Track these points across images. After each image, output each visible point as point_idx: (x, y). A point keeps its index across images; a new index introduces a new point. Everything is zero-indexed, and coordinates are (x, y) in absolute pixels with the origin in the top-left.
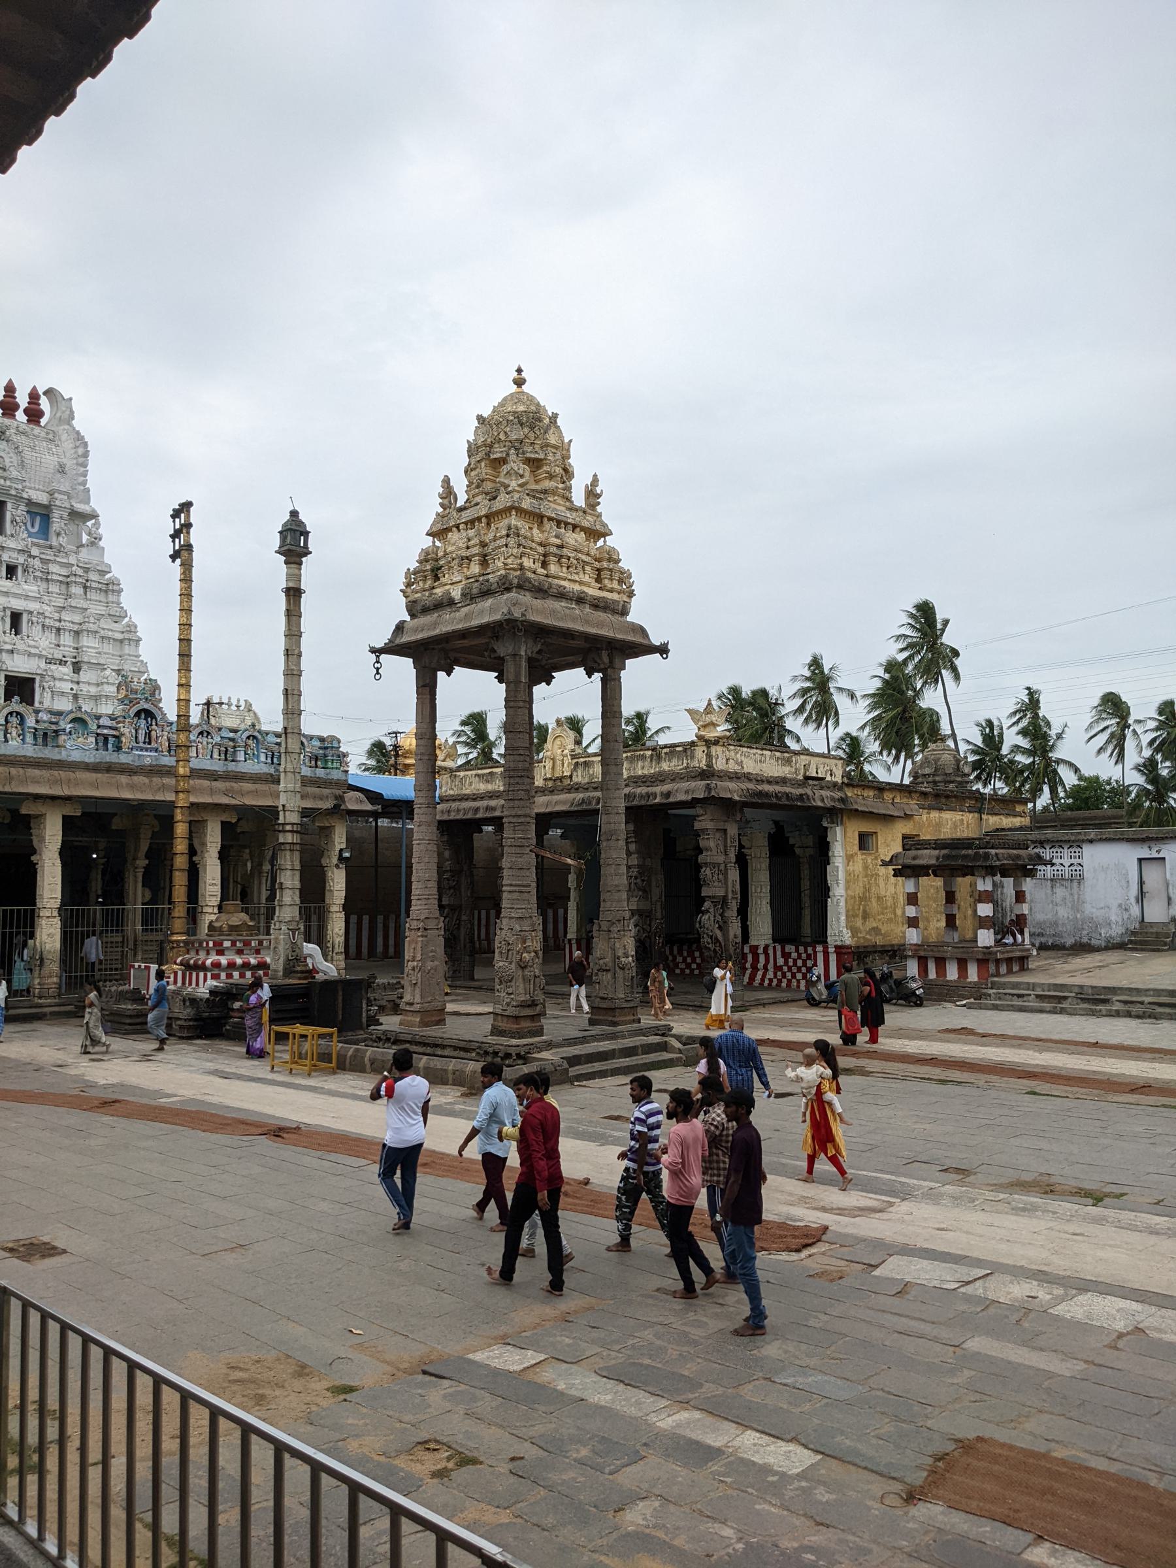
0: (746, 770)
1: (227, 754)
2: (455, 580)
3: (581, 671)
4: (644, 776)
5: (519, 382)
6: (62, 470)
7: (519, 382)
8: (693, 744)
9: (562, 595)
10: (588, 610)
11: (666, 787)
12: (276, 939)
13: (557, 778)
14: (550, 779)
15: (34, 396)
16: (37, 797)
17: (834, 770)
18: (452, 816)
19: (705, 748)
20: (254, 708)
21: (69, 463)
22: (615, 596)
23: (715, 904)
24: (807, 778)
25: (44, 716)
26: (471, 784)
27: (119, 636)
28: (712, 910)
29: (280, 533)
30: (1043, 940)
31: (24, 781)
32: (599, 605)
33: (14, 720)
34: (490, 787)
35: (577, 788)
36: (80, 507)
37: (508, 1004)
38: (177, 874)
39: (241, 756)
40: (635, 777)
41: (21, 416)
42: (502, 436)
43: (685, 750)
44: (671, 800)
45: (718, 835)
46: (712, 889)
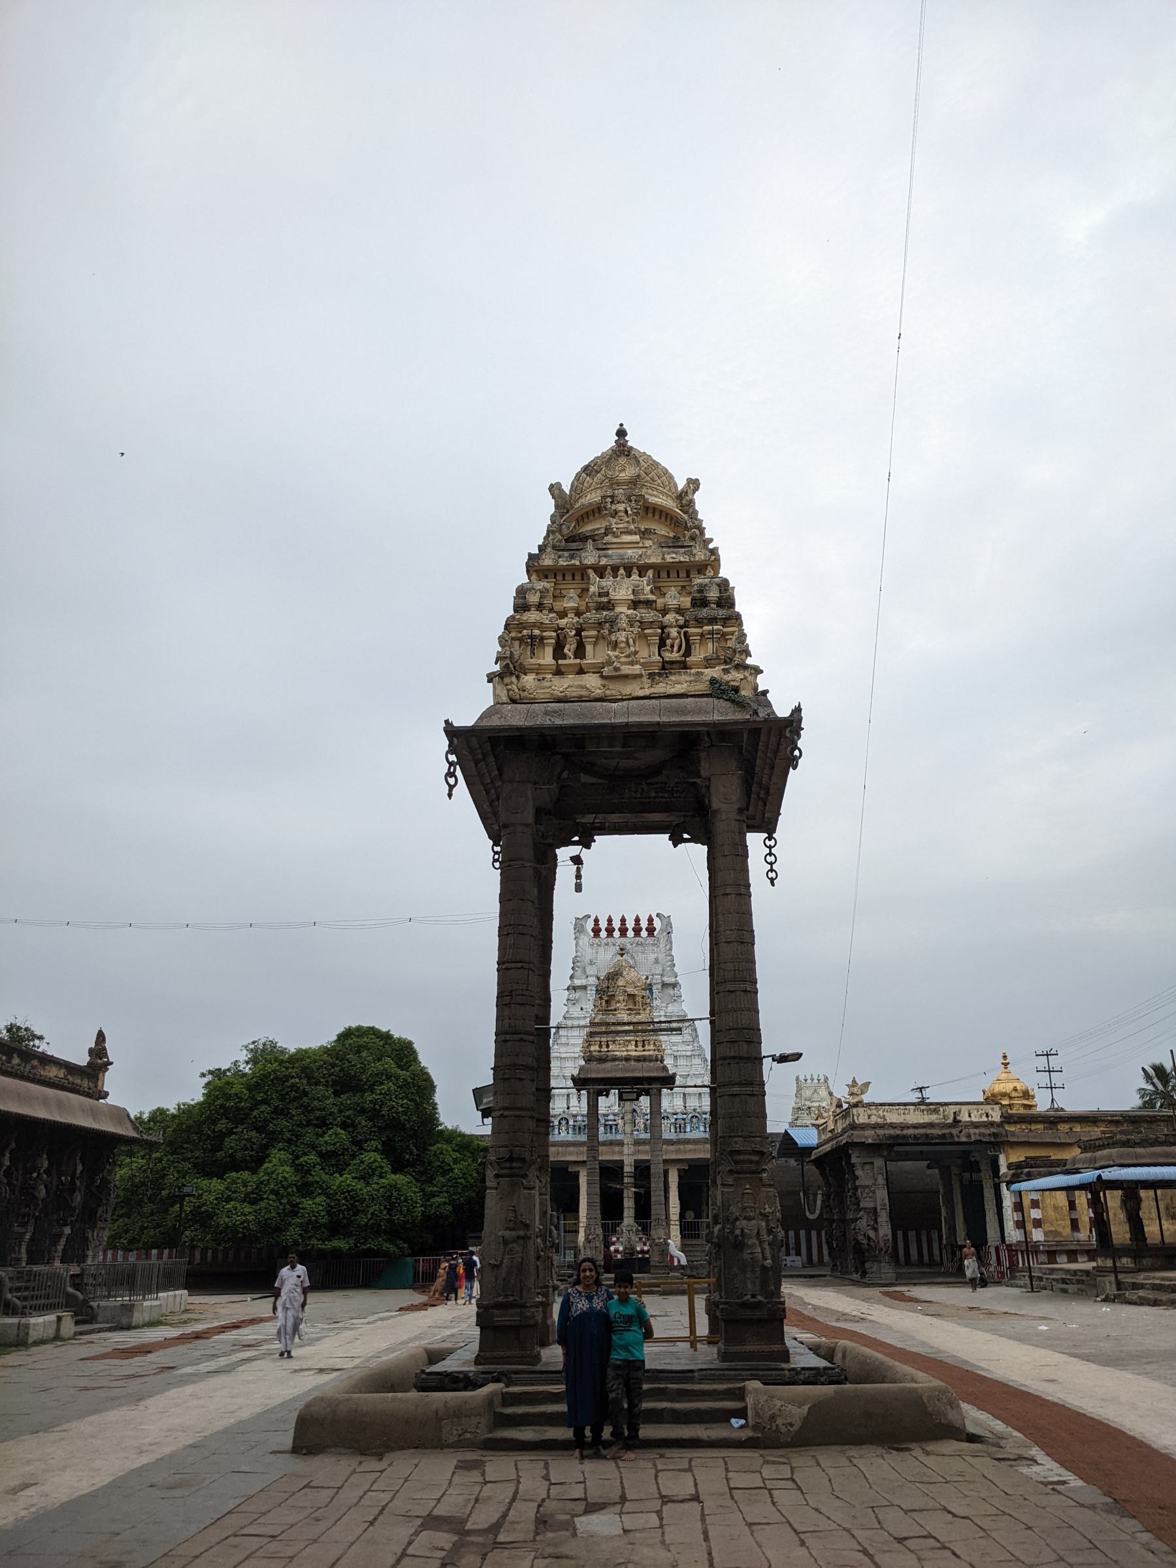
0: (889, 1121)
1: (679, 1128)
6: (657, 961)
9: (615, 1059)
10: (633, 1063)
15: (650, 920)
16: (575, 1162)
17: (990, 1112)
20: (830, 1083)
21: (661, 956)
22: (651, 1053)
23: (868, 1213)
24: (956, 1121)
25: (579, 1118)
27: (689, 1053)
28: (865, 1217)
31: (565, 1155)
32: (638, 1059)
33: (564, 1122)
36: (667, 980)
38: (626, 1200)
39: (688, 1129)
41: (644, 933)
45: (867, 1167)
46: (866, 1203)
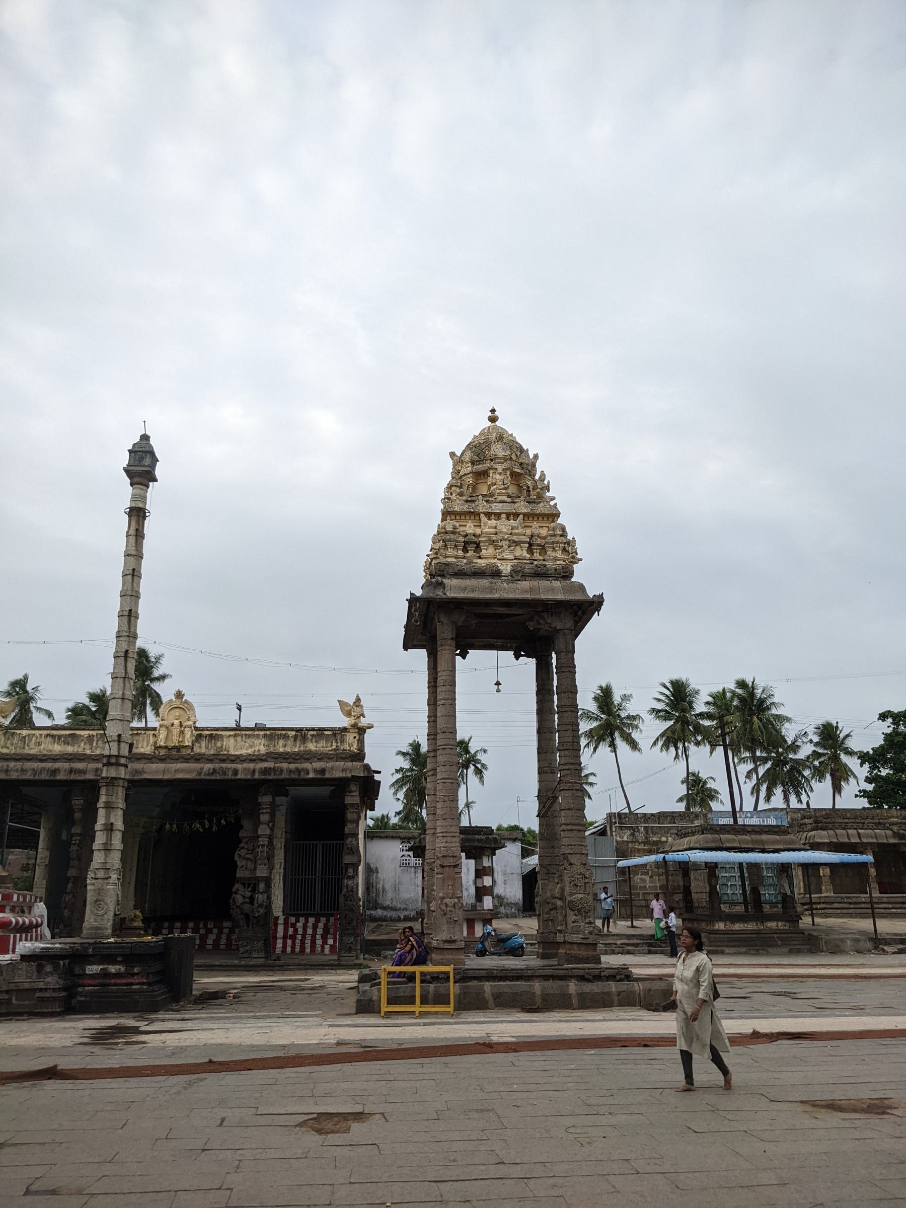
2: (506, 557)
3: (511, 654)
4: (288, 753)
5: (493, 419)
7: (493, 419)
8: (345, 730)
11: (318, 765)
12: (99, 891)
13: (174, 747)
14: (166, 747)
18: (14, 776)
19: (356, 735)
26: (39, 744)
29: (129, 451)
30: (406, 913)
34: (70, 749)
35: (198, 758)
37: (591, 933)
40: (276, 753)
42: (514, 457)
43: (335, 735)
44: (327, 776)
